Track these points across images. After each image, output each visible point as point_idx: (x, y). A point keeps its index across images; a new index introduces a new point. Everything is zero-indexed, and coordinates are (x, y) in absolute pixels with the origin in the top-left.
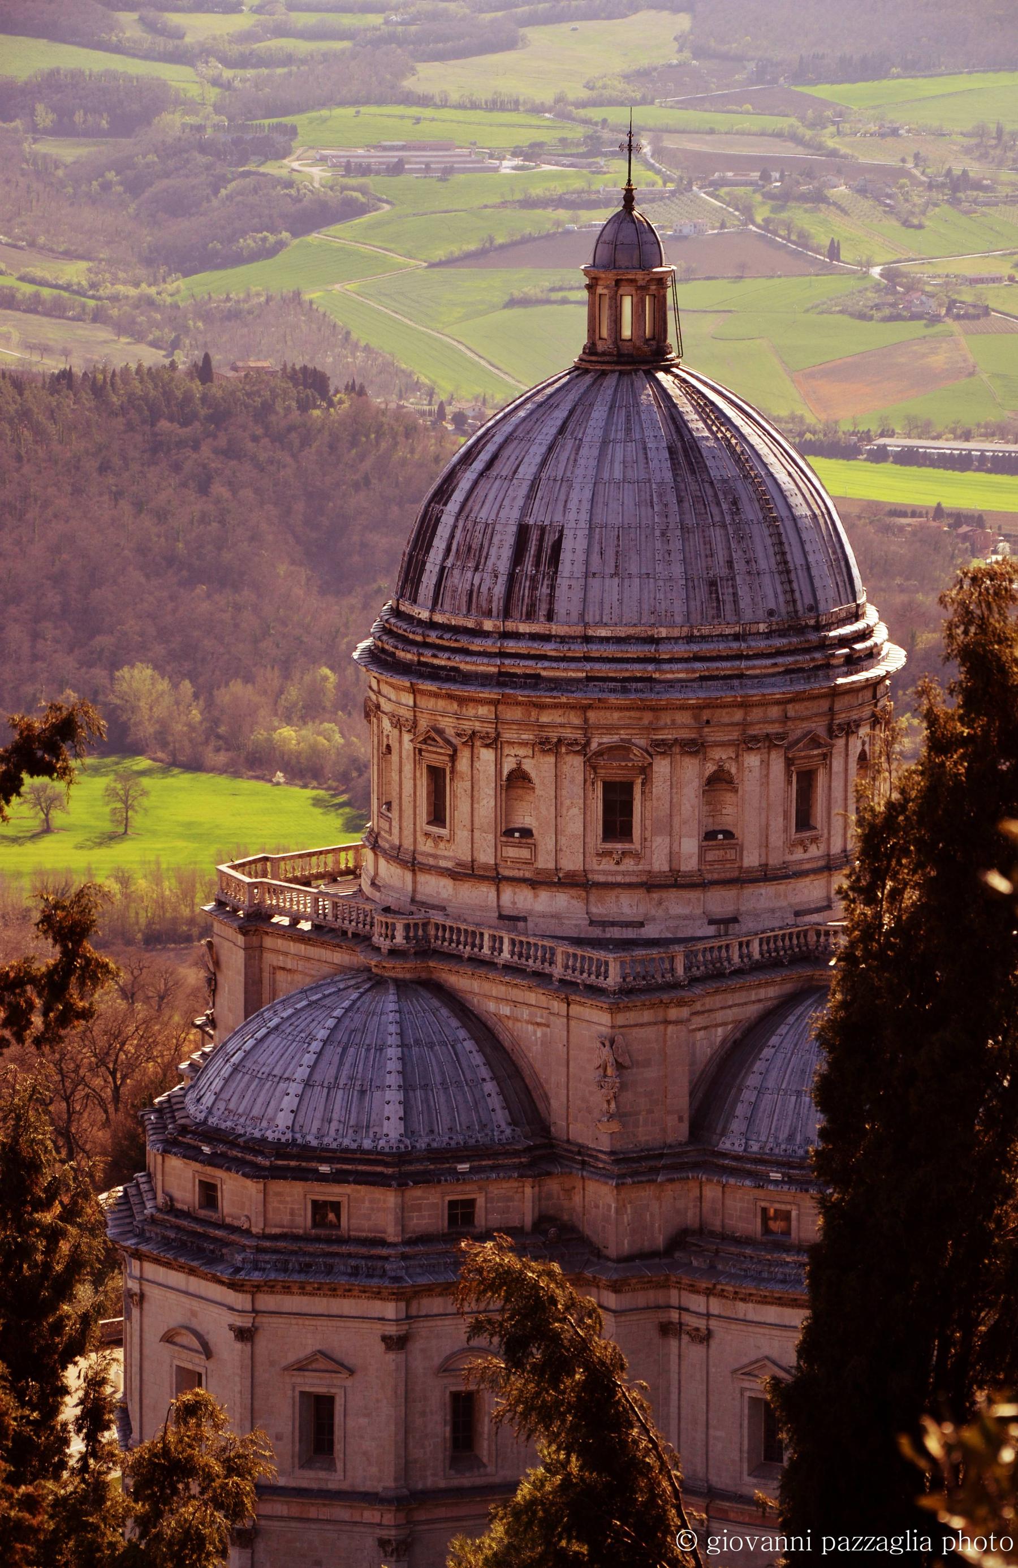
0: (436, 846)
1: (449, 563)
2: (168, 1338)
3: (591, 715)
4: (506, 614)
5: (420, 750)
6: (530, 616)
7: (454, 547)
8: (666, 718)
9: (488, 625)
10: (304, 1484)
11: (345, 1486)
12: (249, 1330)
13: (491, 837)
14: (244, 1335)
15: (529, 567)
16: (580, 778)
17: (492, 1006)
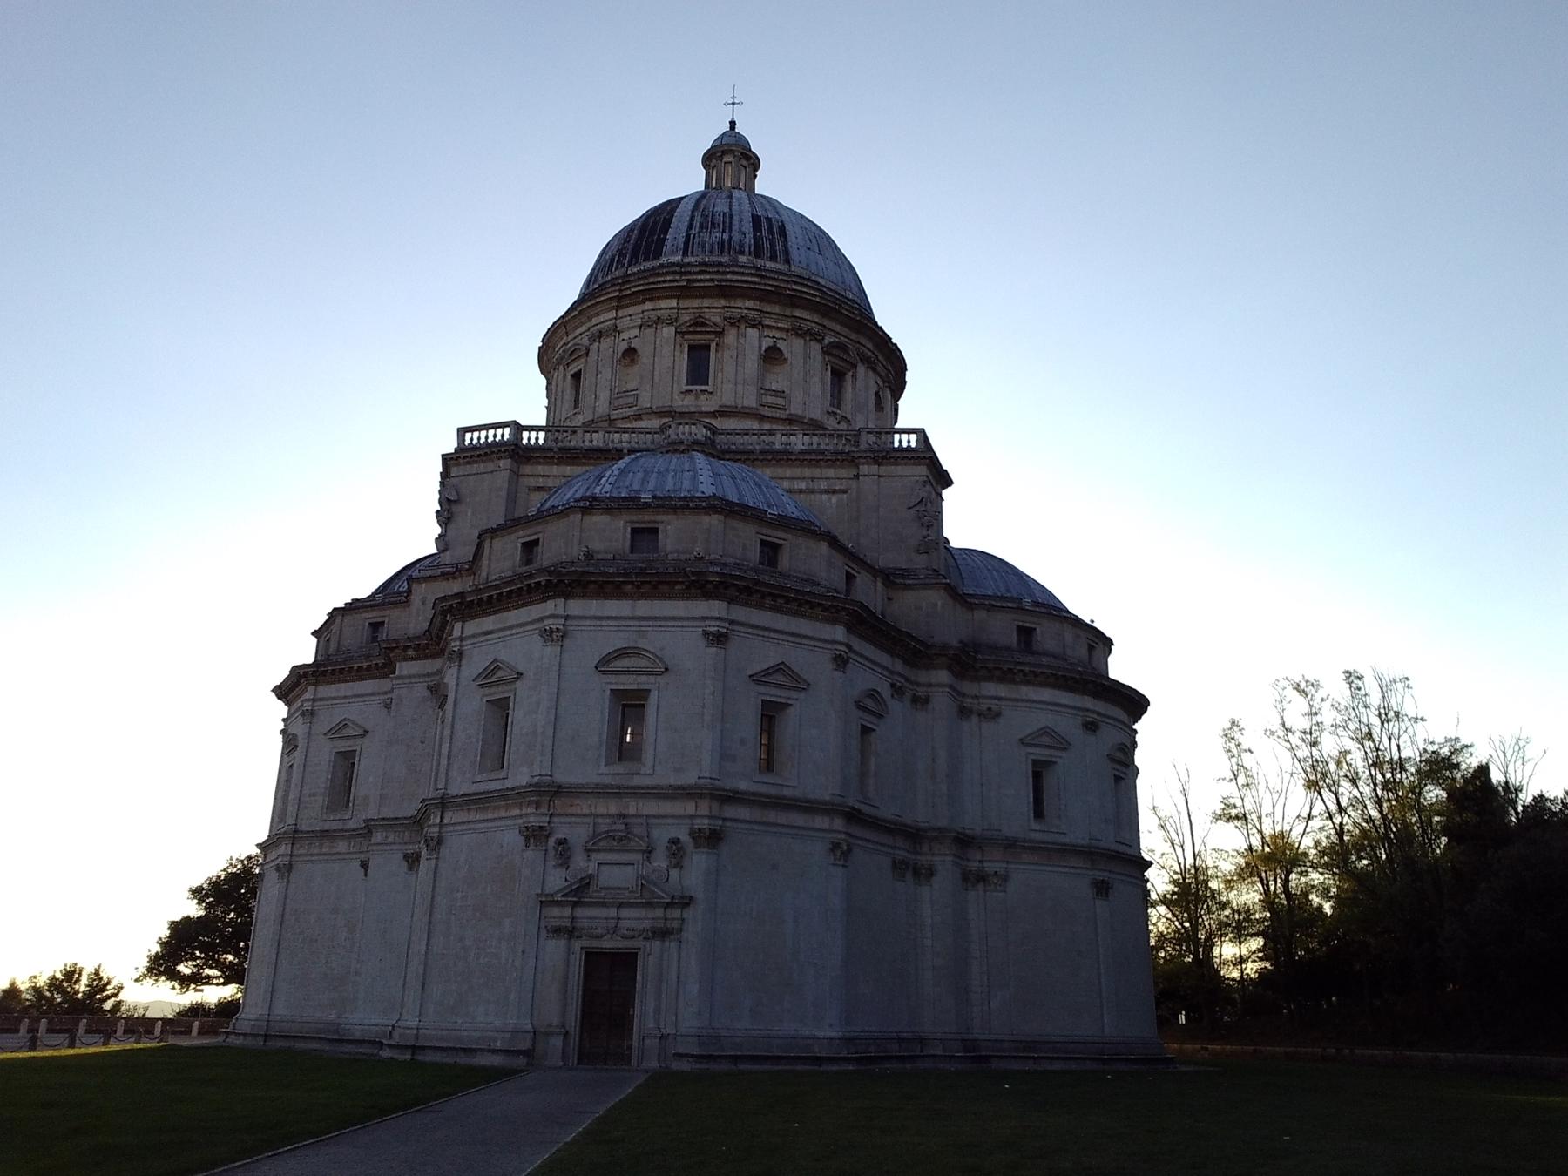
0: (697, 398)
2: (604, 665)
3: (826, 322)
4: (757, 256)
5: (684, 333)
6: (773, 258)
7: (696, 224)
8: (863, 341)
10: (763, 789)
11: (797, 793)
12: (725, 636)
13: (753, 389)
14: (719, 639)
15: (765, 233)
16: (819, 357)
17: (786, 484)
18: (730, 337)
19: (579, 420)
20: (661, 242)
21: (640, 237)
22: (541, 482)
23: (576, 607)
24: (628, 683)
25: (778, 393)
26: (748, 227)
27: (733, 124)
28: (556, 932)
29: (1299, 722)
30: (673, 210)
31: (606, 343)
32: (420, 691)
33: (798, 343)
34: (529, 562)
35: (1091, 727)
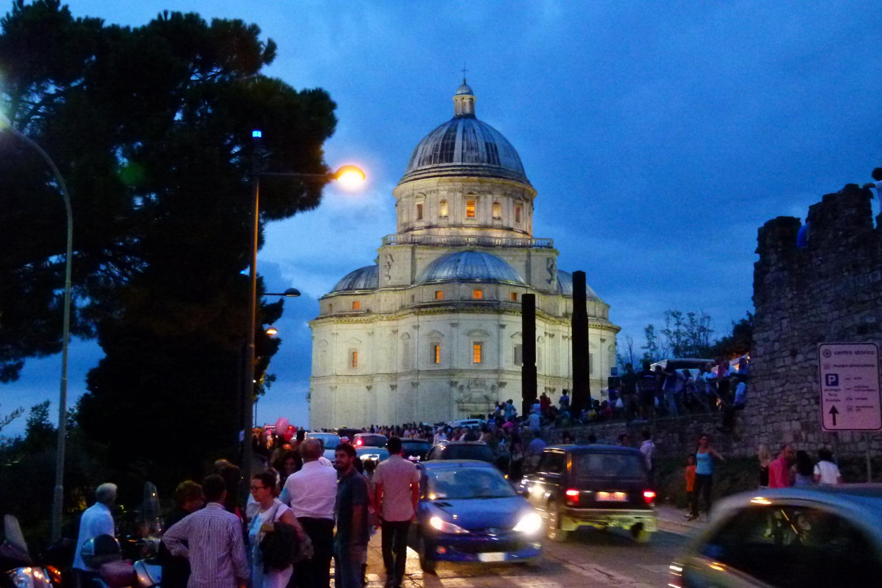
1: (465, 151)
4: (489, 162)
6: (494, 163)
9: (484, 164)
16: (511, 203)
18: (482, 198)
19: (422, 224)
20: (452, 155)
21: (442, 149)
22: (420, 256)
23: (461, 316)
24: (478, 340)
25: (499, 219)
26: (484, 150)
27: (465, 81)
28: (463, 410)
29: (673, 328)
30: (454, 138)
31: (433, 195)
32: (389, 331)
33: (505, 198)
34: (436, 297)
35: (603, 340)
